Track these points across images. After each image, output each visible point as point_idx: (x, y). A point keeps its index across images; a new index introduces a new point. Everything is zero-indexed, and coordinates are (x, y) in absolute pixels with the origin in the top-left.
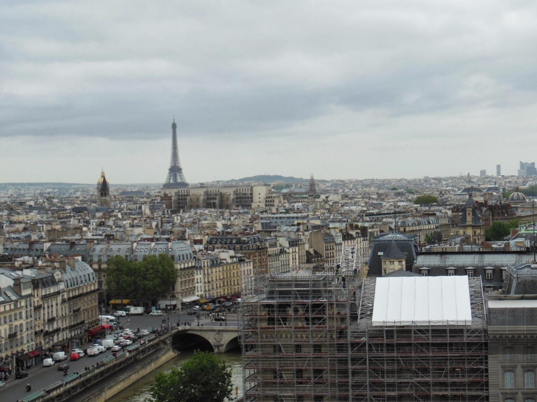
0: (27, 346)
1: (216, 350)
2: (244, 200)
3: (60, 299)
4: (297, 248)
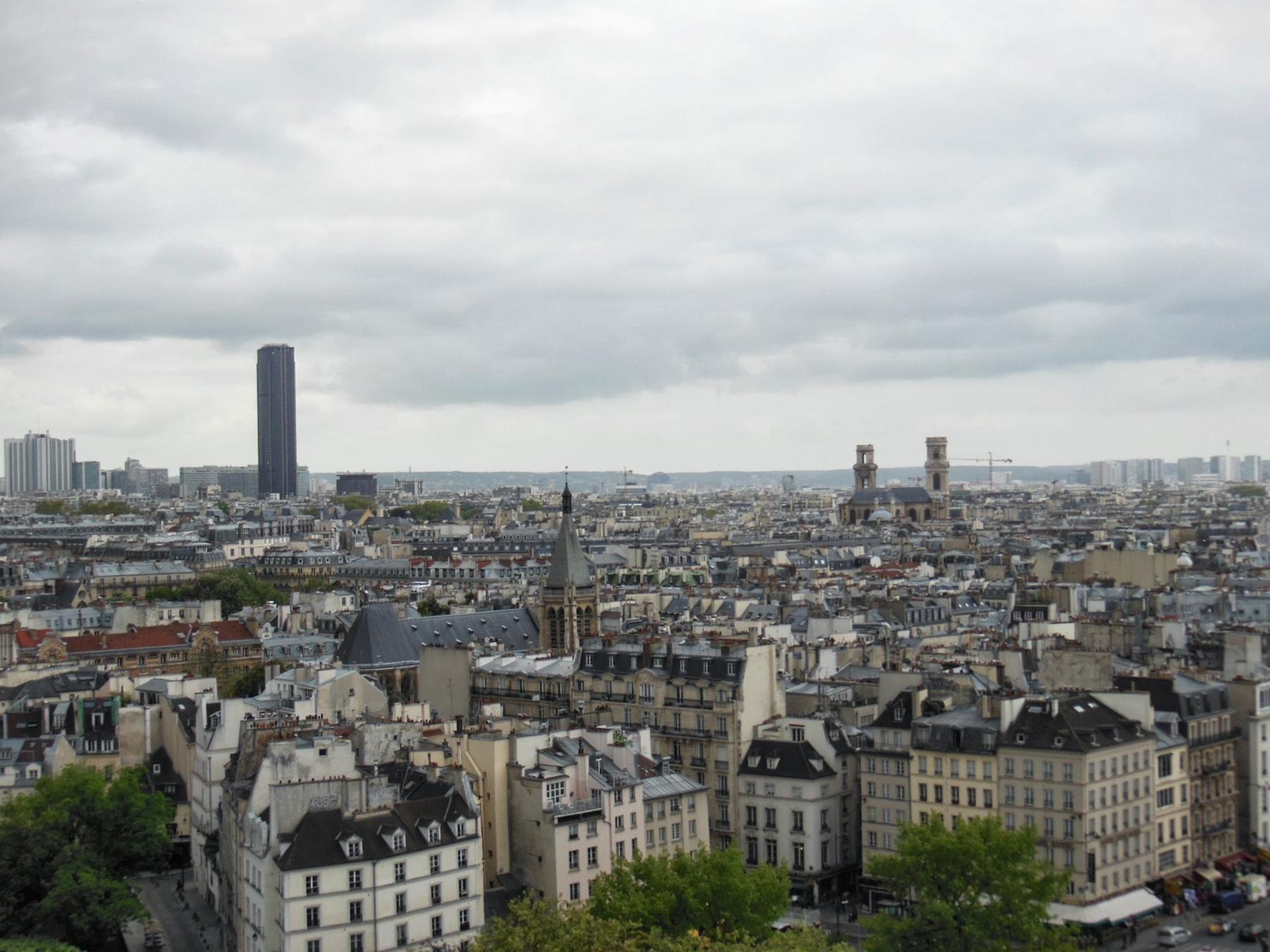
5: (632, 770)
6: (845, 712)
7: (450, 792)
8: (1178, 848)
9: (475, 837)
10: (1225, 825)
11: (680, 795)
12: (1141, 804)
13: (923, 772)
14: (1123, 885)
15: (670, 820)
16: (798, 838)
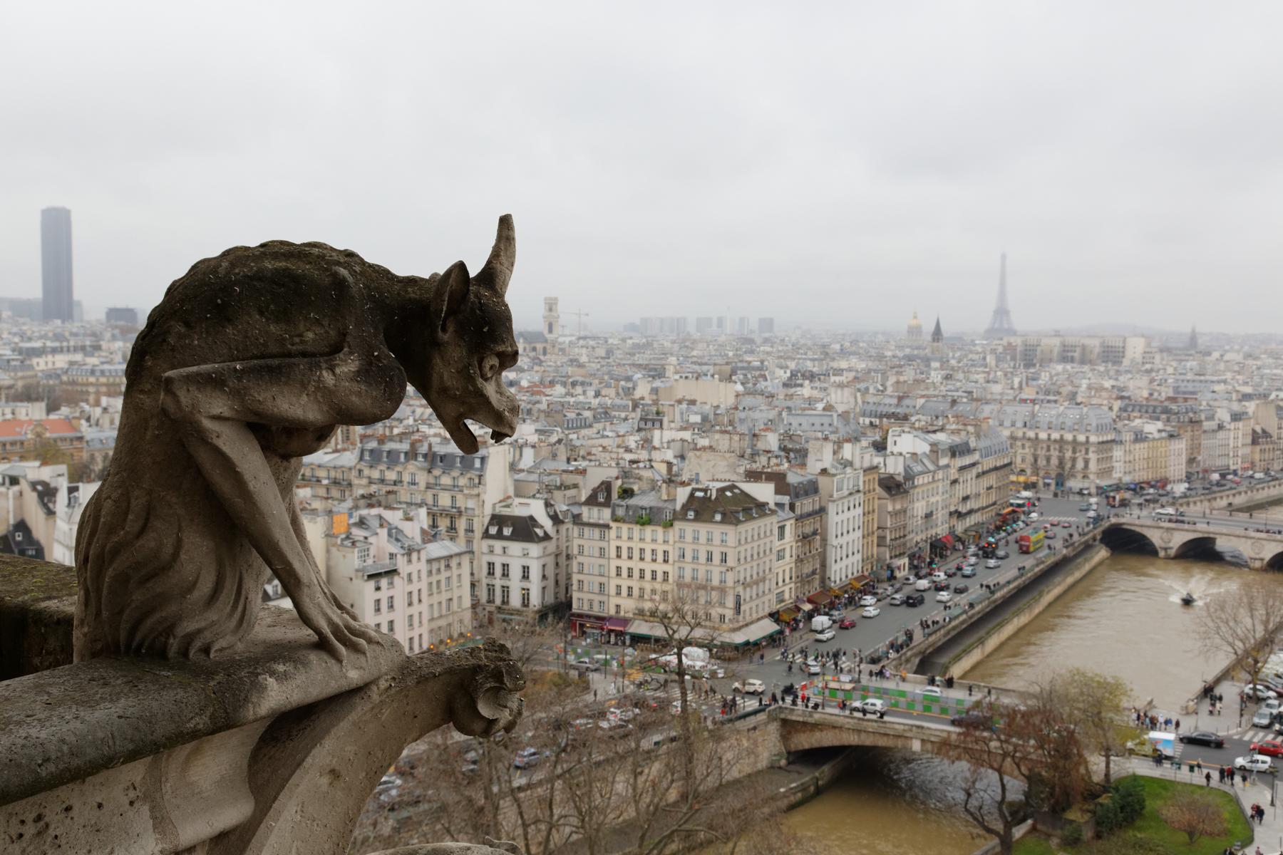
0: (941, 530)
1: (1162, 554)
2: (1112, 355)
3: (974, 471)
4: (1240, 424)
5: (418, 539)
6: (558, 495)
8: (787, 589)
10: (814, 572)
12: (767, 559)
13: (619, 537)
14: (755, 616)
15: (444, 575)
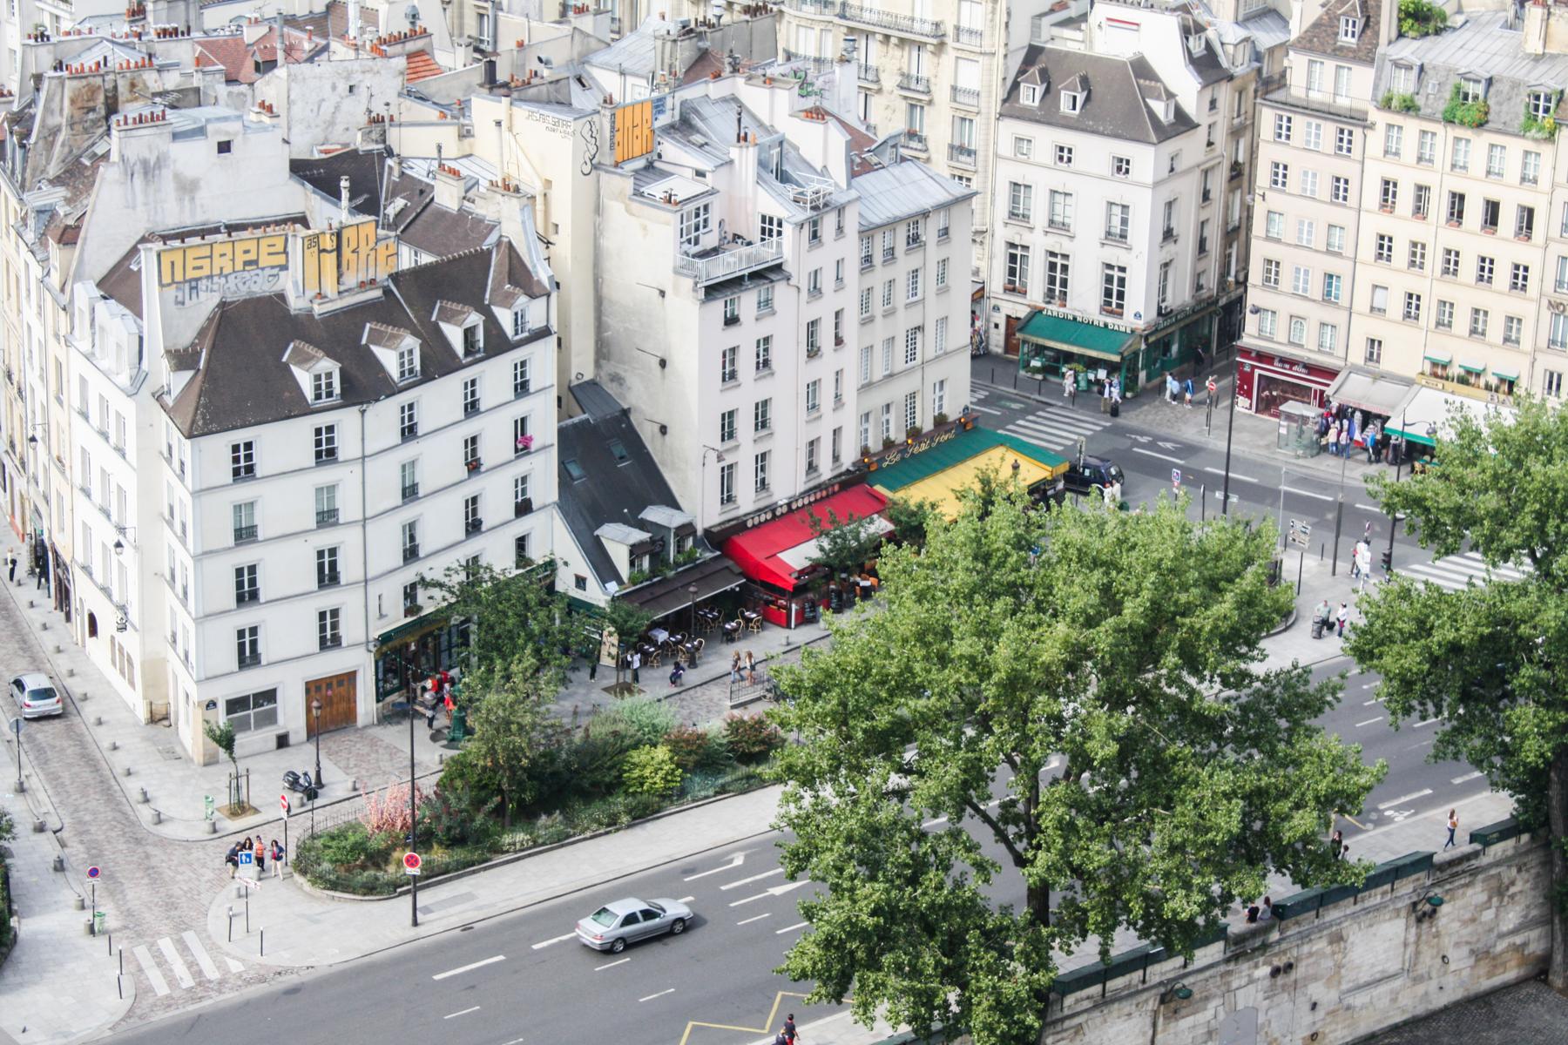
7: (492, 239)
9: (544, 333)
11: (925, 214)
16: (1115, 255)
